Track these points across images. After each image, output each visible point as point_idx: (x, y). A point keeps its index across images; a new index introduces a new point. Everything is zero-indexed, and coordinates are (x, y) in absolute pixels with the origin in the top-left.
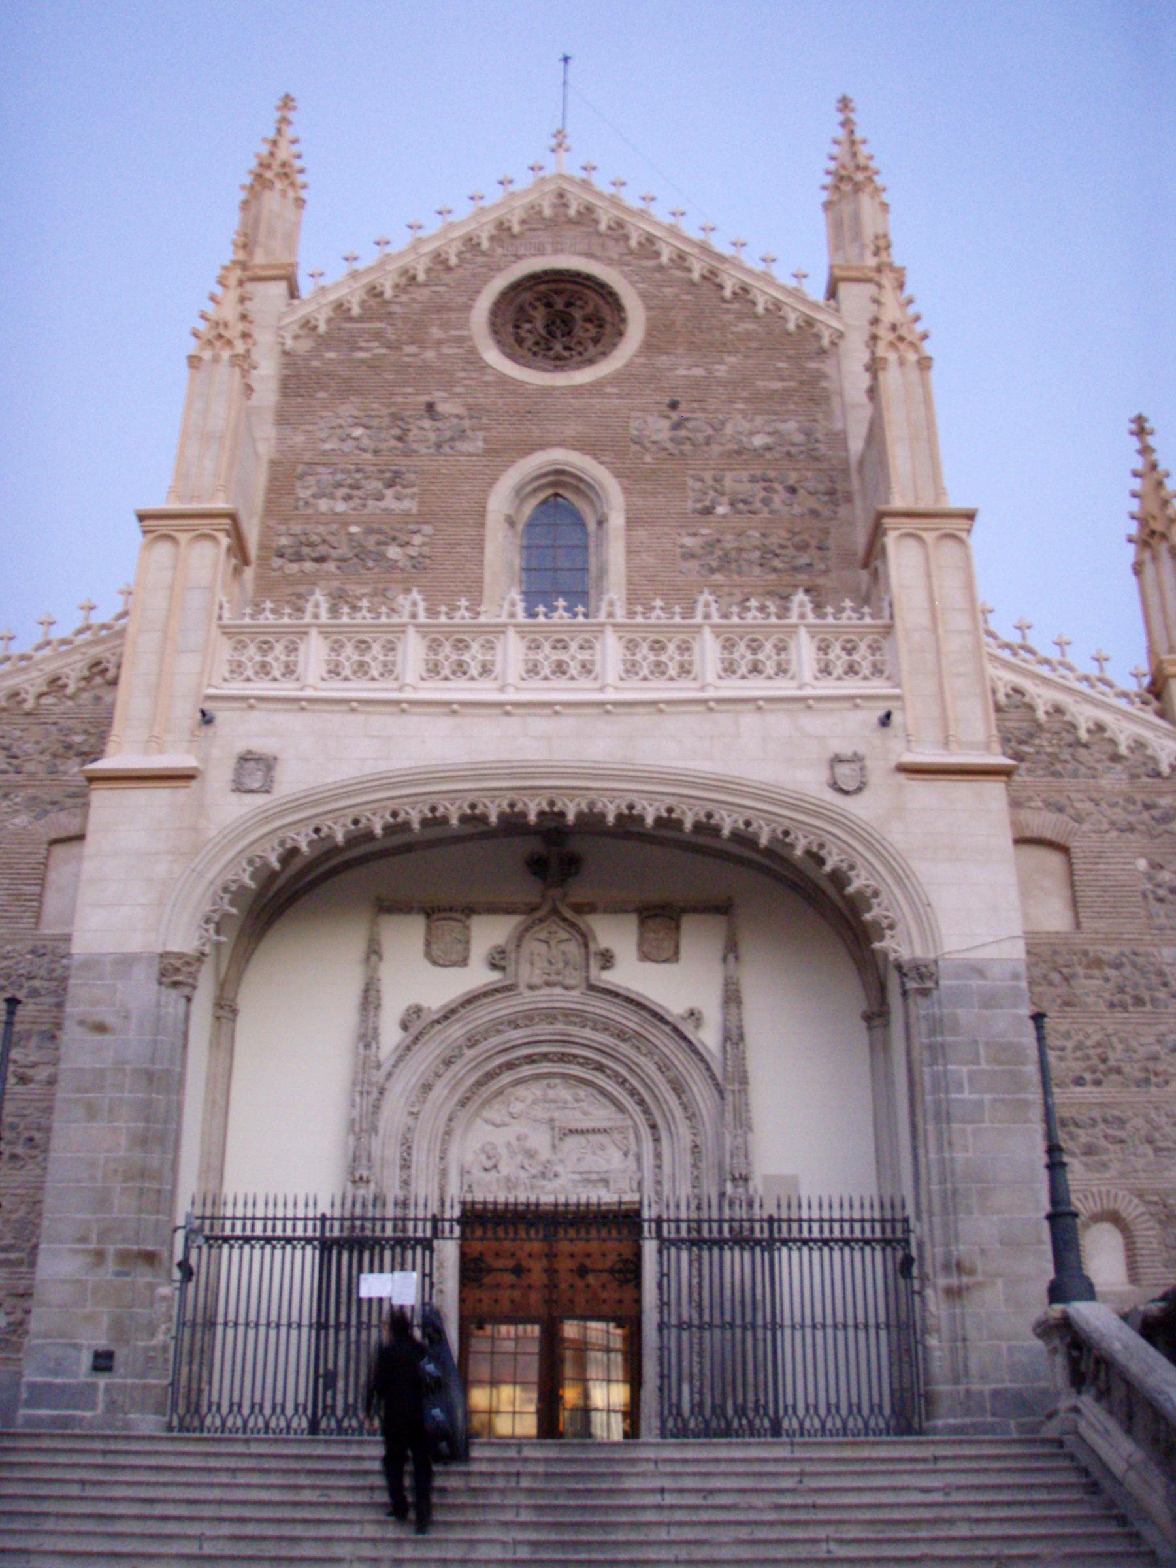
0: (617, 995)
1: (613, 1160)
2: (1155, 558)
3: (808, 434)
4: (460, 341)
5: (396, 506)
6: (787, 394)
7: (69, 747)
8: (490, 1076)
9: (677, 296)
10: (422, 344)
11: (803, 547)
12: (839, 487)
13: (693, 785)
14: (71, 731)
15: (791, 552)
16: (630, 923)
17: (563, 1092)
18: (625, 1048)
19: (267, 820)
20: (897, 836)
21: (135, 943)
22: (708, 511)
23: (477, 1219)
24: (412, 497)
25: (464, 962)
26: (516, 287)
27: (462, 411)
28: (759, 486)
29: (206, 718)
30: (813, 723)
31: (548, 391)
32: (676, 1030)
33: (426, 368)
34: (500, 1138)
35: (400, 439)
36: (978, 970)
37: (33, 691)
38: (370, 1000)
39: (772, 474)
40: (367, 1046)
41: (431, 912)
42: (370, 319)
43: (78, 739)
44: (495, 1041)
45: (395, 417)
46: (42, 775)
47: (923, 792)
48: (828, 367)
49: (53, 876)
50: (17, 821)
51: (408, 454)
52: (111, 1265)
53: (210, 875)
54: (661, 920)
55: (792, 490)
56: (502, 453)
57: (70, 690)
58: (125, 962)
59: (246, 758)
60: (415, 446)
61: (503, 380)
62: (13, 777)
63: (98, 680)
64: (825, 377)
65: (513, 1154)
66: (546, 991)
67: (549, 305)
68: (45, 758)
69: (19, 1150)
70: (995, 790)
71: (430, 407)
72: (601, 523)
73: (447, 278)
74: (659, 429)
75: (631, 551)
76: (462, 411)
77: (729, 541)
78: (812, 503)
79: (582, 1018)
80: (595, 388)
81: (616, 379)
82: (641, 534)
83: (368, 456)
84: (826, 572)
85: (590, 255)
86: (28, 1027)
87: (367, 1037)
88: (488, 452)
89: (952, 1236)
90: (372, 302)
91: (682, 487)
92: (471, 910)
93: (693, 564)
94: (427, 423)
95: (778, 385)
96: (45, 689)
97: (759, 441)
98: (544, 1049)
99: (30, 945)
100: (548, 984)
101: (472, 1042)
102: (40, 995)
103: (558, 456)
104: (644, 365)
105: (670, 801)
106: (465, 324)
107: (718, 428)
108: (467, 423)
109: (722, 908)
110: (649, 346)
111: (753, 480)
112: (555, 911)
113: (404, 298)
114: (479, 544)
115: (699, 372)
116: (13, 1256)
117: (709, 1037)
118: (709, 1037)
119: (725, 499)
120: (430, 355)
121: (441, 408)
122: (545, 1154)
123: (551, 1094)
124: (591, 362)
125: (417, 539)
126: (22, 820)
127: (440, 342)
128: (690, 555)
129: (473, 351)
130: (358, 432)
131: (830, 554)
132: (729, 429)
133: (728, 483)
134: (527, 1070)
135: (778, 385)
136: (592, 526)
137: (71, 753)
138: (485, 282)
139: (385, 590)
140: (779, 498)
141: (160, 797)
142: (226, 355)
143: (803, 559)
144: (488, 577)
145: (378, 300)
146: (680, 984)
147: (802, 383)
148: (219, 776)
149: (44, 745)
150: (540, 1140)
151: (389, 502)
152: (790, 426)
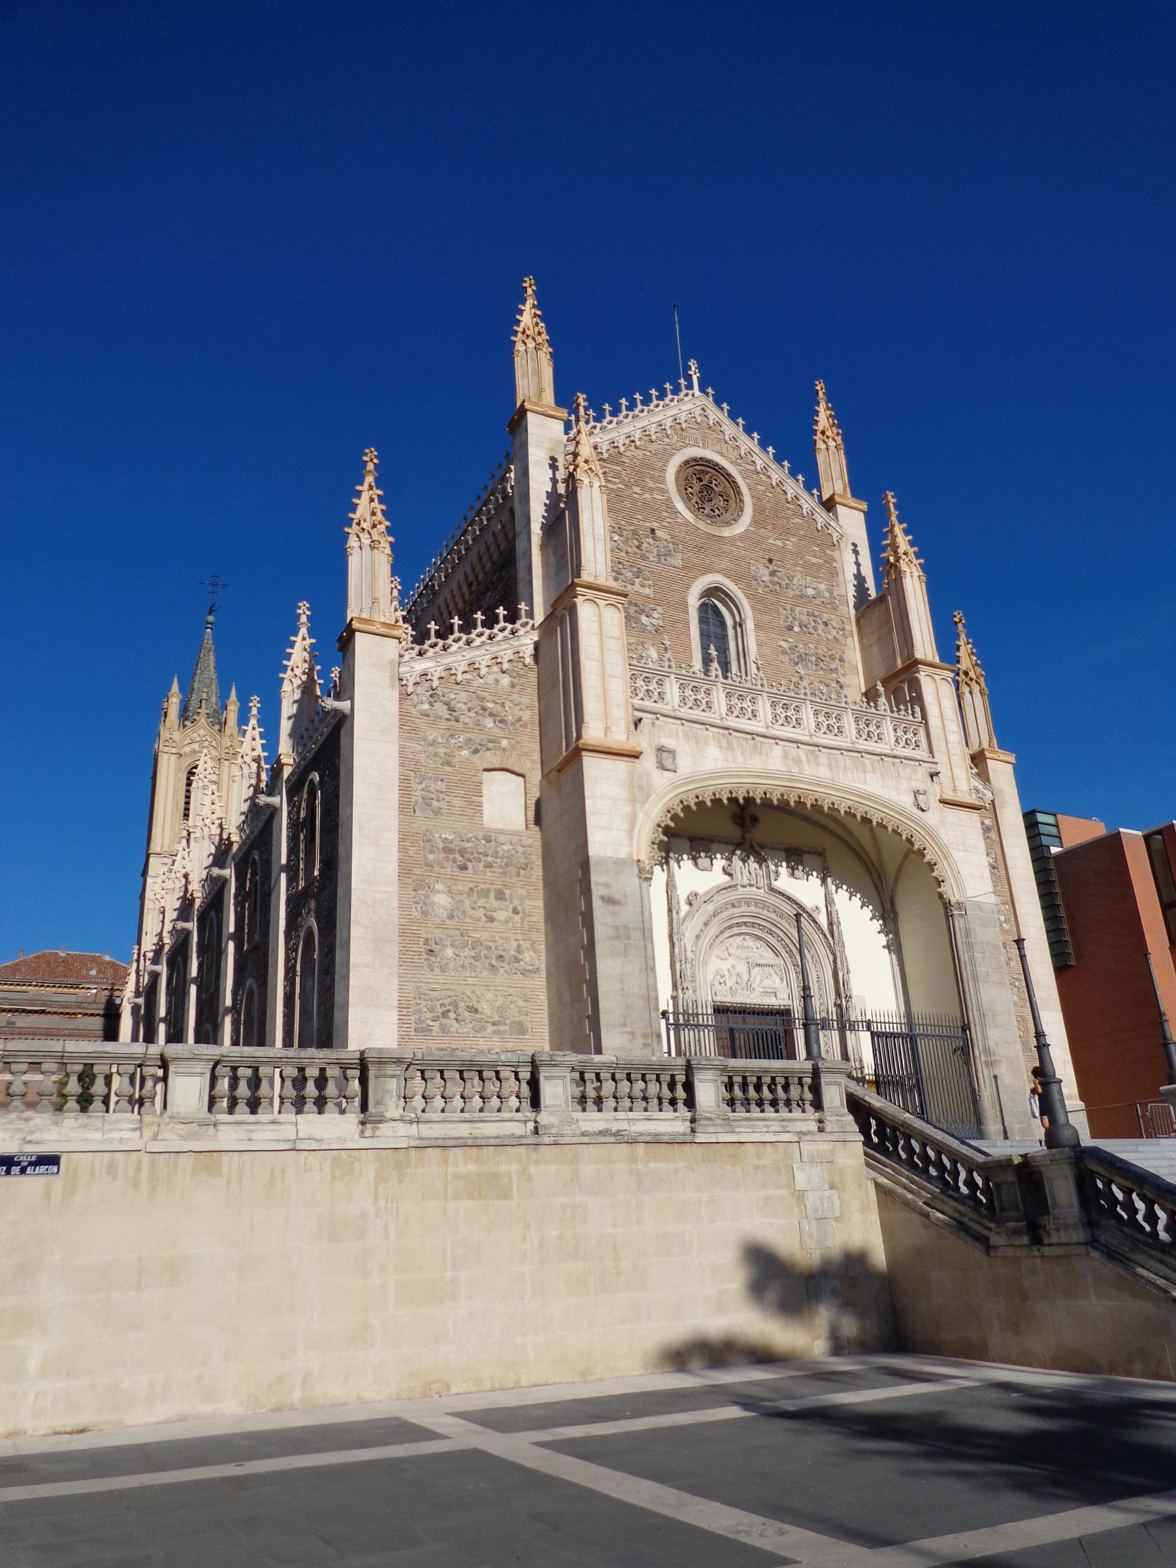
0: (783, 895)
1: (775, 982)
2: (971, 693)
3: (831, 593)
4: (663, 491)
5: (641, 590)
6: (819, 566)
7: (484, 709)
8: (722, 932)
9: (765, 492)
10: (645, 489)
11: (832, 658)
12: (847, 627)
13: (861, 797)
14: (483, 699)
15: (827, 659)
16: (783, 854)
17: (750, 942)
18: (783, 922)
19: (676, 787)
20: (946, 836)
21: (623, 853)
22: (791, 628)
23: (719, 1010)
24: (649, 587)
26: (687, 462)
27: (669, 539)
28: (811, 619)
29: (637, 723)
30: (906, 771)
31: (711, 537)
32: (810, 915)
33: (645, 503)
34: (725, 966)
35: (639, 547)
36: (980, 906)
37: (461, 669)
39: (817, 613)
40: (678, 913)
41: (692, 839)
43: (490, 705)
44: (725, 914)
45: (635, 533)
46: (471, 725)
47: (952, 814)
48: (836, 555)
49: (484, 791)
50: (462, 753)
52: (640, 1041)
53: (652, 816)
54: (795, 856)
55: (826, 624)
56: (692, 571)
57: (483, 671)
58: (620, 863)
59: (661, 750)
60: (647, 554)
61: (687, 523)
62: (453, 723)
63: (496, 668)
64: (834, 560)
65: (731, 975)
66: (748, 888)
67: (700, 480)
68: (472, 714)
69: (494, 962)
70: (975, 816)
71: (653, 531)
73: (652, 447)
74: (764, 573)
75: (759, 645)
76: (669, 539)
77: (801, 649)
78: (834, 632)
79: (763, 904)
80: (732, 540)
81: (743, 537)
82: (763, 636)
83: (623, 554)
84: (844, 675)
85: (722, 454)
86: (488, 886)
88: (684, 567)
89: (985, 1038)
90: (613, 451)
91: (777, 611)
92: (712, 841)
93: (785, 659)
94: (651, 541)
95: (815, 560)
96: (466, 669)
97: (810, 592)
98: (745, 920)
99: (481, 834)
100: (751, 885)
101: (715, 914)
102: (491, 866)
104: (754, 533)
105: (849, 803)
106: (662, 480)
107: (791, 579)
108: (671, 546)
109: (820, 854)
110: (755, 521)
111: (808, 614)
112: (752, 846)
113: (628, 454)
114: (687, 622)
115: (779, 543)
116: (502, 1028)
117: (822, 919)
118: (822, 919)
119: (797, 623)
120: (647, 496)
121: (658, 533)
122: (745, 977)
123: (745, 944)
124: (728, 523)
125: (656, 615)
126: (465, 753)
127: (652, 489)
128: (784, 652)
129: (669, 499)
130: (616, 538)
131: (846, 665)
132: (795, 581)
133: (797, 612)
134: (736, 930)
135: (815, 560)
136: (729, 622)
137: (487, 713)
138: (672, 455)
139: (643, 644)
140: (821, 627)
141: (621, 766)
142: (596, 484)
143: (833, 666)
144: (693, 646)
145: (616, 450)
146: (807, 889)
147: (826, 562)
149: (469, 705)
150: (742, 968)
152: (822, 587)
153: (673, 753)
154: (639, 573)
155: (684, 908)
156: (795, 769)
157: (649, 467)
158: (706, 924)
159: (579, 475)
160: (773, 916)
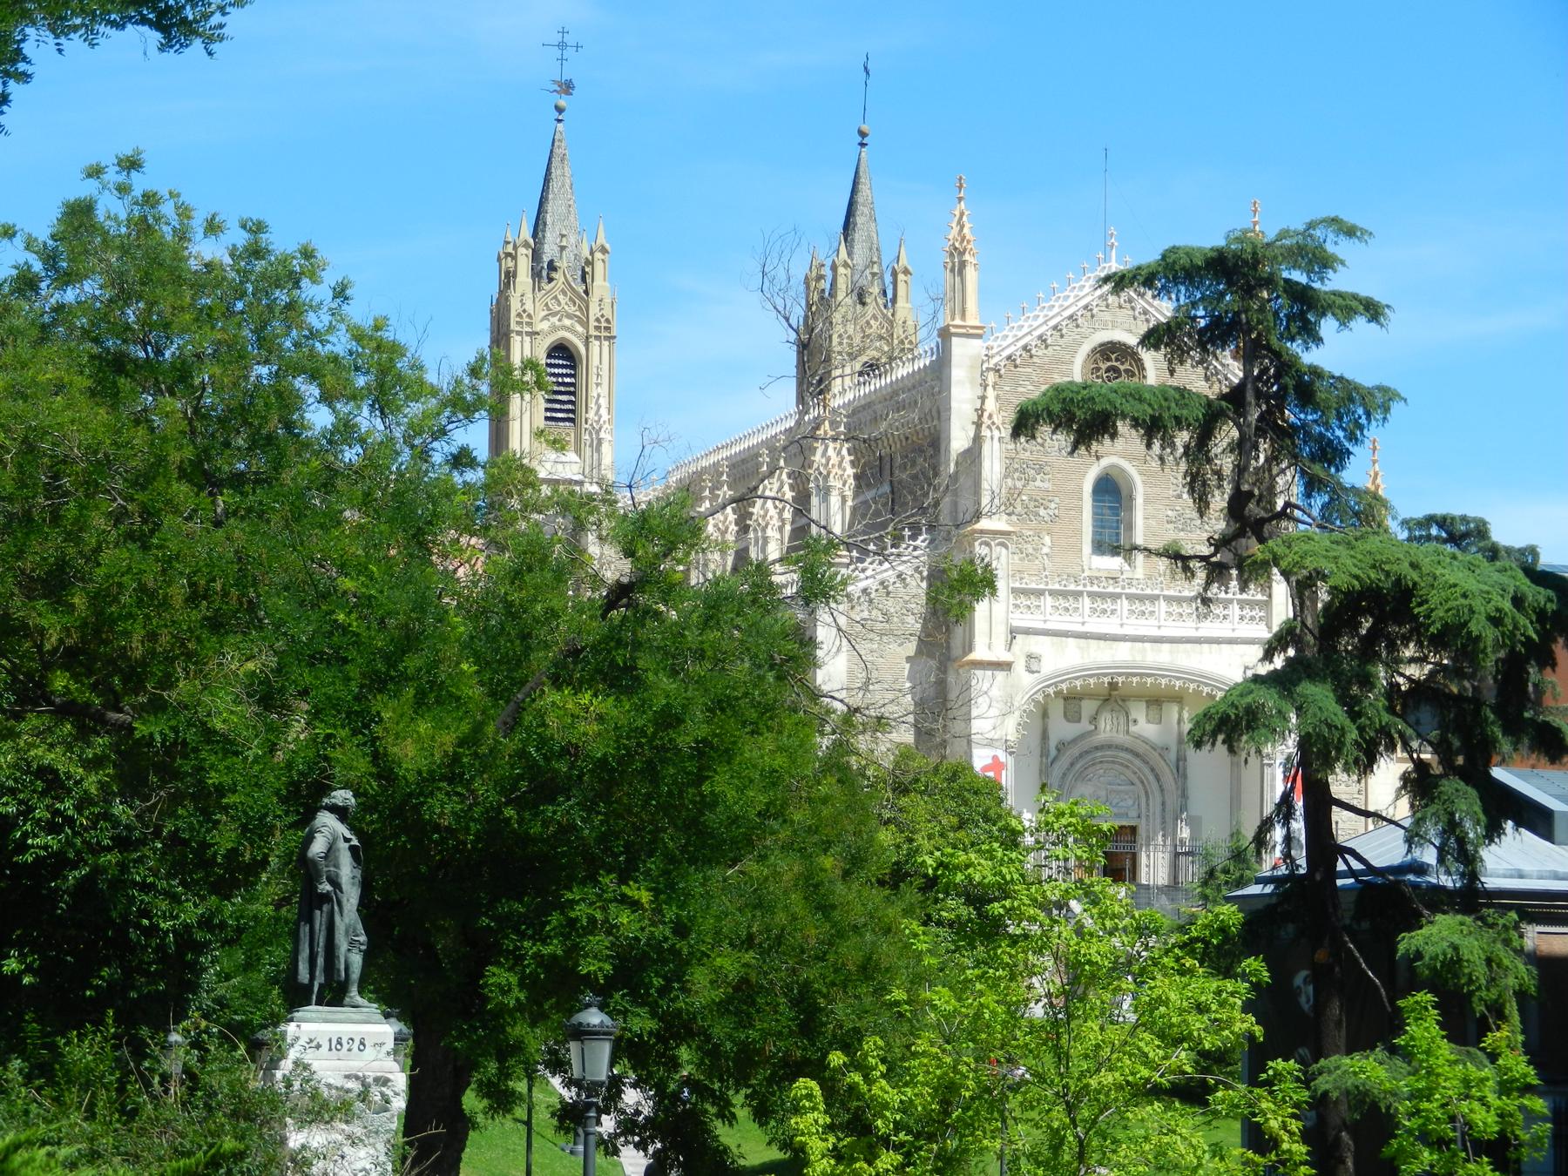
25: (1079, 721)
26: (1094, 350)
38: (1045, 736)
42: (1024, 366)
51: (1046, 453)
59: (1030, 657)
72: (1131, 498)
73: (1061, 342)
87: (1044, 752)
92: (1080, 699)
93: (1171, 526)
103: (1113, 460)
117: (1173, 756)
125: (1053, 505)
136: (1124, 493)
148: (1020, 666)
151: (1038, 483)
153: (1038, 658)
154: (1040, 470)
155: (1053, 752)
156: (1138, 658)
157: (1060, 361)
158: (1072, 764)
159: (985, 432)
160: (1129, 756)
